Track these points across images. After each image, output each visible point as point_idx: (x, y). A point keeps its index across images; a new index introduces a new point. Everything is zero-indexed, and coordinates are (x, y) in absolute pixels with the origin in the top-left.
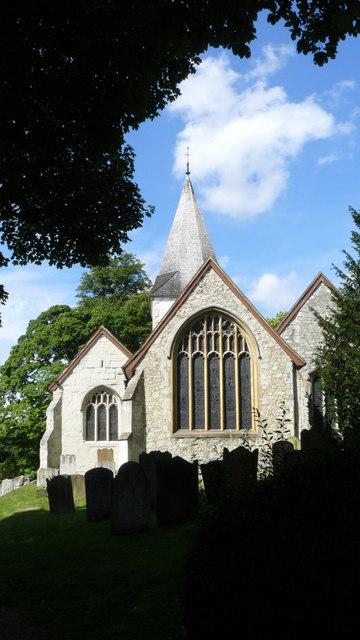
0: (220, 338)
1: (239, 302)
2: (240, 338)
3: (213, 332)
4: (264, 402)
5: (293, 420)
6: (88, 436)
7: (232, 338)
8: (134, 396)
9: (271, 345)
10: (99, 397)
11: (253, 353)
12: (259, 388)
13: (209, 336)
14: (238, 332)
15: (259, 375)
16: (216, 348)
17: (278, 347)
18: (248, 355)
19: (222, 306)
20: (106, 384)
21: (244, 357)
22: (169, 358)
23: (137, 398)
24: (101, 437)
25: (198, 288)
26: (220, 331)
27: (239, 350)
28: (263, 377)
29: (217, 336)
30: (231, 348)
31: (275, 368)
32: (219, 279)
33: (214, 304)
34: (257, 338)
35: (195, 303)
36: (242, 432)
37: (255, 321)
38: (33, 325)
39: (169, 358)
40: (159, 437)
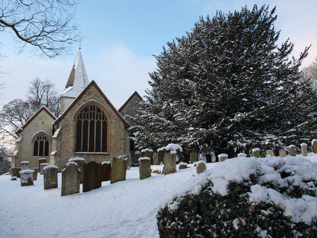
2: (104, 115)
3: (93, 112)
6: (35, 154)
11: (109, 121)
13: (91, 113)
15: (111, 130)
17: (119, 119)
21: (105, 124)
24: (41, 155)
27: (103, 119)
28: (112, 131)
29: (94, 113)
30: (100, 119)
37: (110, 107)
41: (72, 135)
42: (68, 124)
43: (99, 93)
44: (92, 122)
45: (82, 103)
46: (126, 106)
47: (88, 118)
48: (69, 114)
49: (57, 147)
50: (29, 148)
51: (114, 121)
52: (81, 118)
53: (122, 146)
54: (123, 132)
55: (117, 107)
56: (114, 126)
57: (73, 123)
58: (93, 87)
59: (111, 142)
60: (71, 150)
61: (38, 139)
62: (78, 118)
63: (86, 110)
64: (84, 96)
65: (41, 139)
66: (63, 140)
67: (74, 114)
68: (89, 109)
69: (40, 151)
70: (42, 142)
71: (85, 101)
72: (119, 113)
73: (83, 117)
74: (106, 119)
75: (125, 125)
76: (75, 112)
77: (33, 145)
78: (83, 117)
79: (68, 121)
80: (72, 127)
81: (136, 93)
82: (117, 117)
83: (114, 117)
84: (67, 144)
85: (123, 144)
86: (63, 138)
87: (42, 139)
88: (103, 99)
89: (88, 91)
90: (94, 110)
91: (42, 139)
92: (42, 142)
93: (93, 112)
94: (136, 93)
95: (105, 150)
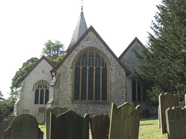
0: (94, 61)
1: (103, 46)
2: (103, 61)
3: (91, 58)
4: (113, 89)
5: (125, 97)
6: (36, 102)
7: (99, 61)
8: (55, 84)
9: (116, 64)
10: (41, 85)
12: (111, 83)
14: (103, 59)
15: (111, 77)
16: (93, 65)
17: (119, 65)
18: (106, 69)
19: (96, 47)
20: (44, 80)
21: (105, 71)
22: (71, 68)
23: (57, 85)
24: (41, 103)
25: (85, 39)
26: (95, 58)
27: (103, 66)
28: (113, 78)
29: (93, 59)
31: (118, 74)
32: (94, 35)
33: (92, 46)
34: (110, 61)
35: (84, 45)
36: (103, 101)
37: (109, 54)
38: (24, 64)
39: (71, 68)
40: (66, 103)
41: (70, 83)
42: (66, 71)
43: (97, 39)
44: (91, 69)
45: (80, 48)
46: (127, 53)
47: (86, 65)
48: (66, 61)
49: (54, 95)
50: (30, 96)
51: (114, 68)
52: (79, 65)
53: (124, 95)
54: (124, 80)
55: (118, 56)
56: (114, 73)
57: (71, 70)
58: (92, 32)
59: (112, 91)
60: (69, 99)
61: (39, 87)
62: (76, 65)
63: (85, 56)
64: (82, 42)
65: (41, 87)
66: (60, 88)
67: (72, 61)
68: (88, 56)
69: (40, 99)
70: (42, 91)
71: (83, 46)
72: (119, 60)
73: (81, 64)
74: (106, 66)
75: (126, 72)
76: (72, 59)
77: (34, 93)
78: (81, 64)
79: (66, 68)
80: (70, 75)
81: (136, 40)
82: (117, 63)
83: (115, 63)
84: (64, 92)
85: (125, 93)
86: (61, 86)
87: (42, 88)
88: (102, 44)
89: (86, 37)
90: (93, 57)
91: (42, 88)
92: (42, 91)
93: (91, 58)
94: (136, 40)
95: (105, 97)
